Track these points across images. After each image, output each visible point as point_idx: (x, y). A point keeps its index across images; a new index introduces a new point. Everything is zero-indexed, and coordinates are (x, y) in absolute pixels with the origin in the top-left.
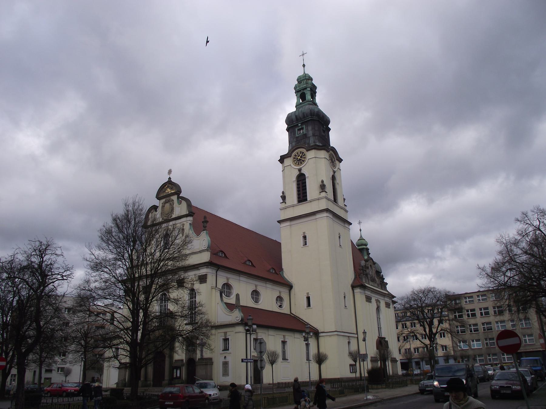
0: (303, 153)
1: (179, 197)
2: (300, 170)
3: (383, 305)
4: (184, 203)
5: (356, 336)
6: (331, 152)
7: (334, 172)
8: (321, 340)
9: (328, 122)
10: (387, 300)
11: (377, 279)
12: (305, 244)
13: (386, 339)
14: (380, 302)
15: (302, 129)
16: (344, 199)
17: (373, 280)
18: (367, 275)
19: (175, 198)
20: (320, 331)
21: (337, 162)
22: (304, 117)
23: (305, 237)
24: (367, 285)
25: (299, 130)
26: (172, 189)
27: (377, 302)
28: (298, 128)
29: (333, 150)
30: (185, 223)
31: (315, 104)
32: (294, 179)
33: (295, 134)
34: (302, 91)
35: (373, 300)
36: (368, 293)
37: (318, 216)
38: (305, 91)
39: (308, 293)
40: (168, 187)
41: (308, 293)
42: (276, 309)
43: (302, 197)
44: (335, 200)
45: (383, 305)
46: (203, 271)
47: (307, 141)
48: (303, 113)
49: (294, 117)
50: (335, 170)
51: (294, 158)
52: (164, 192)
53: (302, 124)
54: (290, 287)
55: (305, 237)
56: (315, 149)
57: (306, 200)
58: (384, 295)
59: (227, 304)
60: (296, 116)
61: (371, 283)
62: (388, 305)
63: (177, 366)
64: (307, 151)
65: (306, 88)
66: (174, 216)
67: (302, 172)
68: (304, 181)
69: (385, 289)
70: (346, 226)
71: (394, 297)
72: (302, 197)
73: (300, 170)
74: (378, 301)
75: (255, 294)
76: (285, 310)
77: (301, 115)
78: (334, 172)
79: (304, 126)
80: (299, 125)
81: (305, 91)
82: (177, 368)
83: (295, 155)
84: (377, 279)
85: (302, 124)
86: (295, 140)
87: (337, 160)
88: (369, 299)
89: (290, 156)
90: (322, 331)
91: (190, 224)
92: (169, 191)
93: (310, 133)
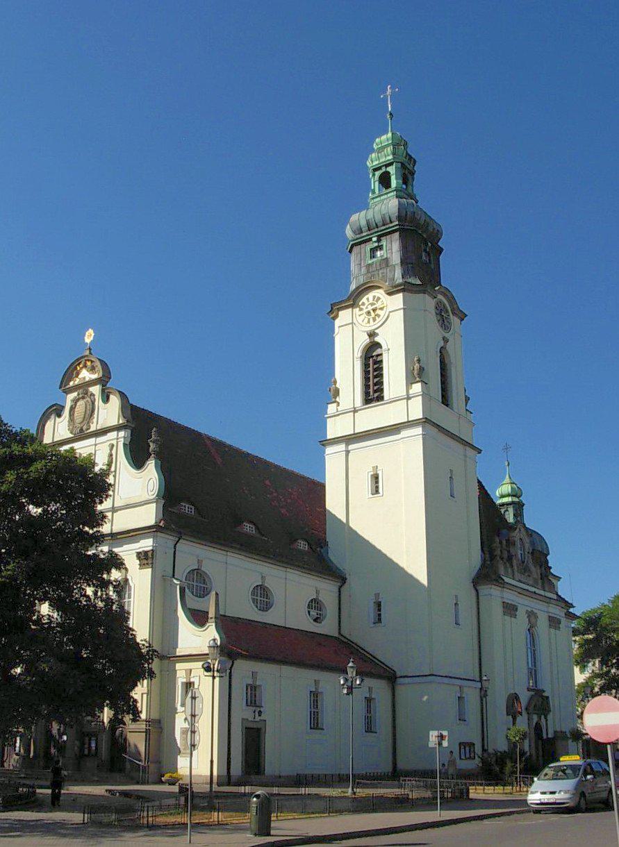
0: (379, 299)
1: (103, 391)
2: (372, 335)
3: (543, 623)
4: (115, 401)
5: (479, 685)
6: (440, 297)
7: (446, 340)
8: (404, 691)
9: (437, 235)
10: (558, 612)
11: (533, 568)
12: (376, 491)
13: (545, 694)
14: (536, 617)
15: (380, 248)
16: (467, 399)
17: (525, 570)
18: (510, 558)
19: (96, 390)
20: (399, 674)
21: (455, 320)
23: (376, 478)
24: (507, 580)
26: (93, 369)
27: (529, 617)
29: (446, 293)
30: (114, 442)
31: (412, 197)
32: (358, 354)
34: (384, 169)
35: (521, 613)
36: (510, 597)
37: (405, 433)
38: (389, 169)
39: (377, 595)
40: (85, 366)
41: (377, 595)
42: (308, 625)
43: (373, 391)
44: (445, 400)
45: (543, 623)
46: (147, 544)
47: (390, 275)
50: (446, 335)
54: (341, 579)
55: (376, 478)
56: (403, 290)
57: (380, 398)
58: (548, 600)
59: (189, 609)
61: (517, 575)
62: (554, 622)
64: (390, 294)
65: (391, 164)
66: (93, 428)
67: (377, 339)
68: (379, 359)
69: (553, 588)
70: (470, 452)
71: (571, 606)
72: (373, 391)
73: (372, 335)
74: (531, 615)
75: (262, 596)
76: (328, 627)
77: (378, 219)
78: (446, 340)
80: (375, 239)
81: (389, 169)
84: (533, 568)
86: (364, 270)
87: (454, 314)
88: (510, 609)
90: (402, 674)
91: (125, 445)
93: (396, 258)
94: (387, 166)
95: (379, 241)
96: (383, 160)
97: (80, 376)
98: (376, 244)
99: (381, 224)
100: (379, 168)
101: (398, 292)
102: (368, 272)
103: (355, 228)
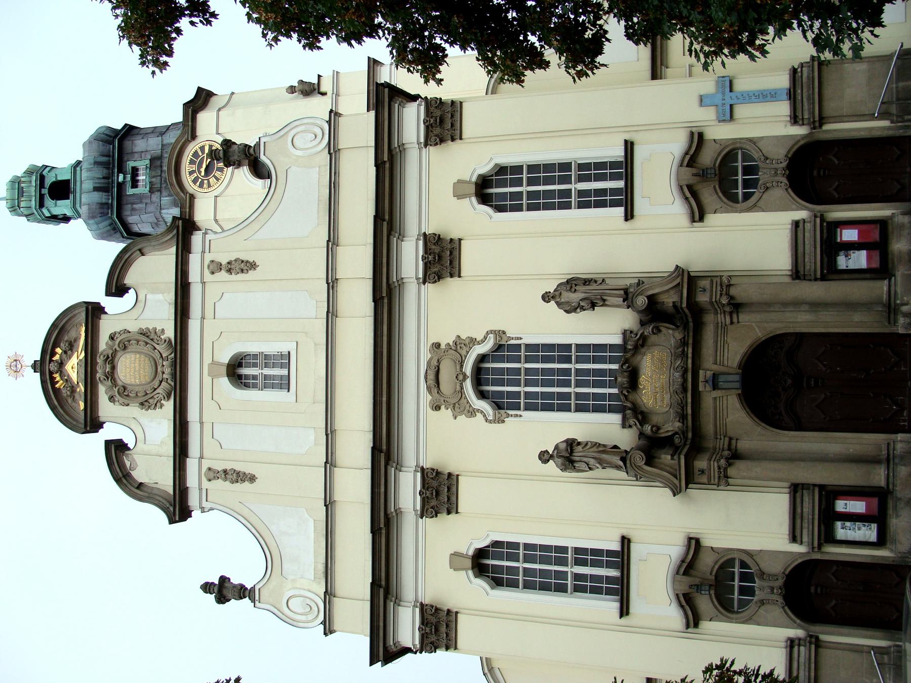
0: (196, 154)
15: (135, 171)
22: (106, 165)
25: (135, 184)
28: (129, 185)
33: (140, 198)
34: (45, 191)
40: (61, 364)
48: (96, 163)
49: (97, 197)
51: (201, 186)
52: (73, 390)
53: (121, 170)
56: (195, 112)
60: (96, 189)
63: (819, 255)
64: (194, 137)
77: (99, 173)
79: (131, 164)
82: (831, 247)
83: (195, 181)
85: (121, 170)
89: (192, 197)
92: (73, 367)
94: (42, 185)
95: (125, 174)
96: (33, 203)
97: (74, 376)
98: (129, 177)
99: (105, 171)
100: (42, 197)
101: (194, 120)
102: (160, 191)
103: (98, 211)
